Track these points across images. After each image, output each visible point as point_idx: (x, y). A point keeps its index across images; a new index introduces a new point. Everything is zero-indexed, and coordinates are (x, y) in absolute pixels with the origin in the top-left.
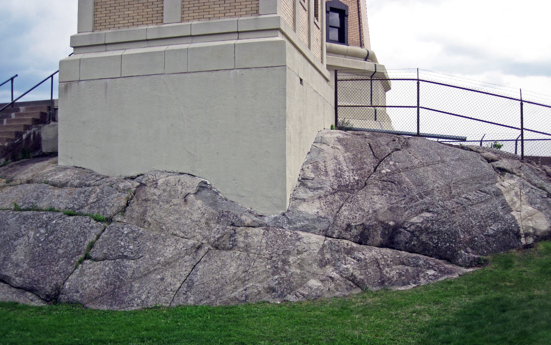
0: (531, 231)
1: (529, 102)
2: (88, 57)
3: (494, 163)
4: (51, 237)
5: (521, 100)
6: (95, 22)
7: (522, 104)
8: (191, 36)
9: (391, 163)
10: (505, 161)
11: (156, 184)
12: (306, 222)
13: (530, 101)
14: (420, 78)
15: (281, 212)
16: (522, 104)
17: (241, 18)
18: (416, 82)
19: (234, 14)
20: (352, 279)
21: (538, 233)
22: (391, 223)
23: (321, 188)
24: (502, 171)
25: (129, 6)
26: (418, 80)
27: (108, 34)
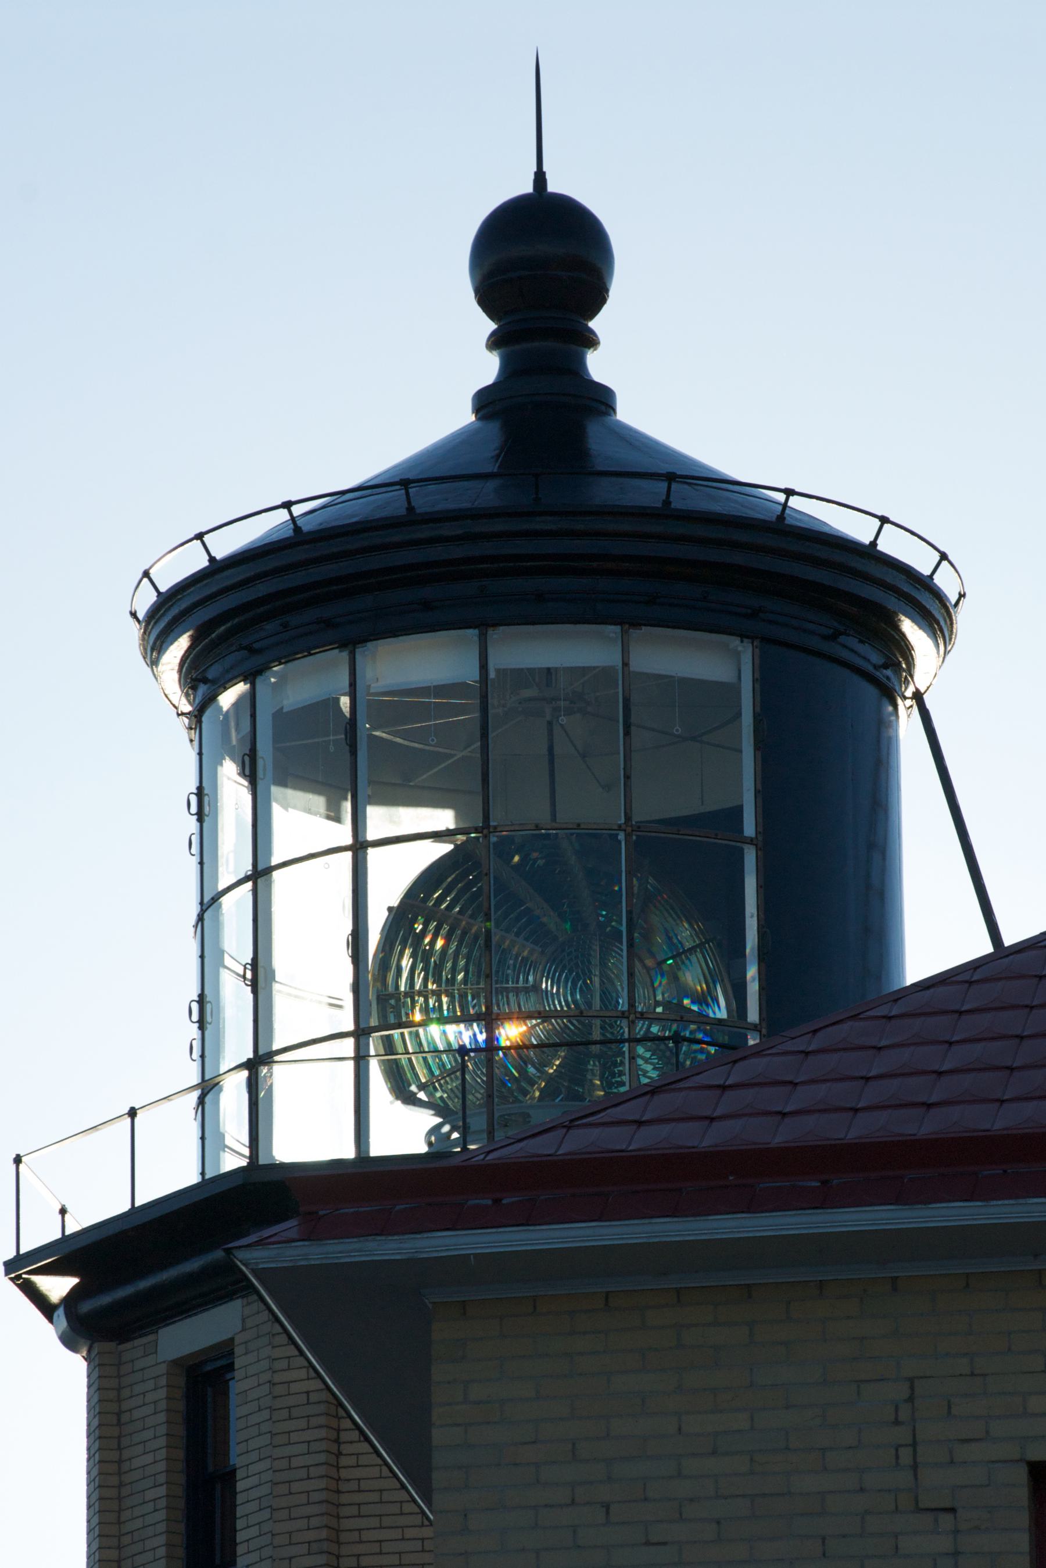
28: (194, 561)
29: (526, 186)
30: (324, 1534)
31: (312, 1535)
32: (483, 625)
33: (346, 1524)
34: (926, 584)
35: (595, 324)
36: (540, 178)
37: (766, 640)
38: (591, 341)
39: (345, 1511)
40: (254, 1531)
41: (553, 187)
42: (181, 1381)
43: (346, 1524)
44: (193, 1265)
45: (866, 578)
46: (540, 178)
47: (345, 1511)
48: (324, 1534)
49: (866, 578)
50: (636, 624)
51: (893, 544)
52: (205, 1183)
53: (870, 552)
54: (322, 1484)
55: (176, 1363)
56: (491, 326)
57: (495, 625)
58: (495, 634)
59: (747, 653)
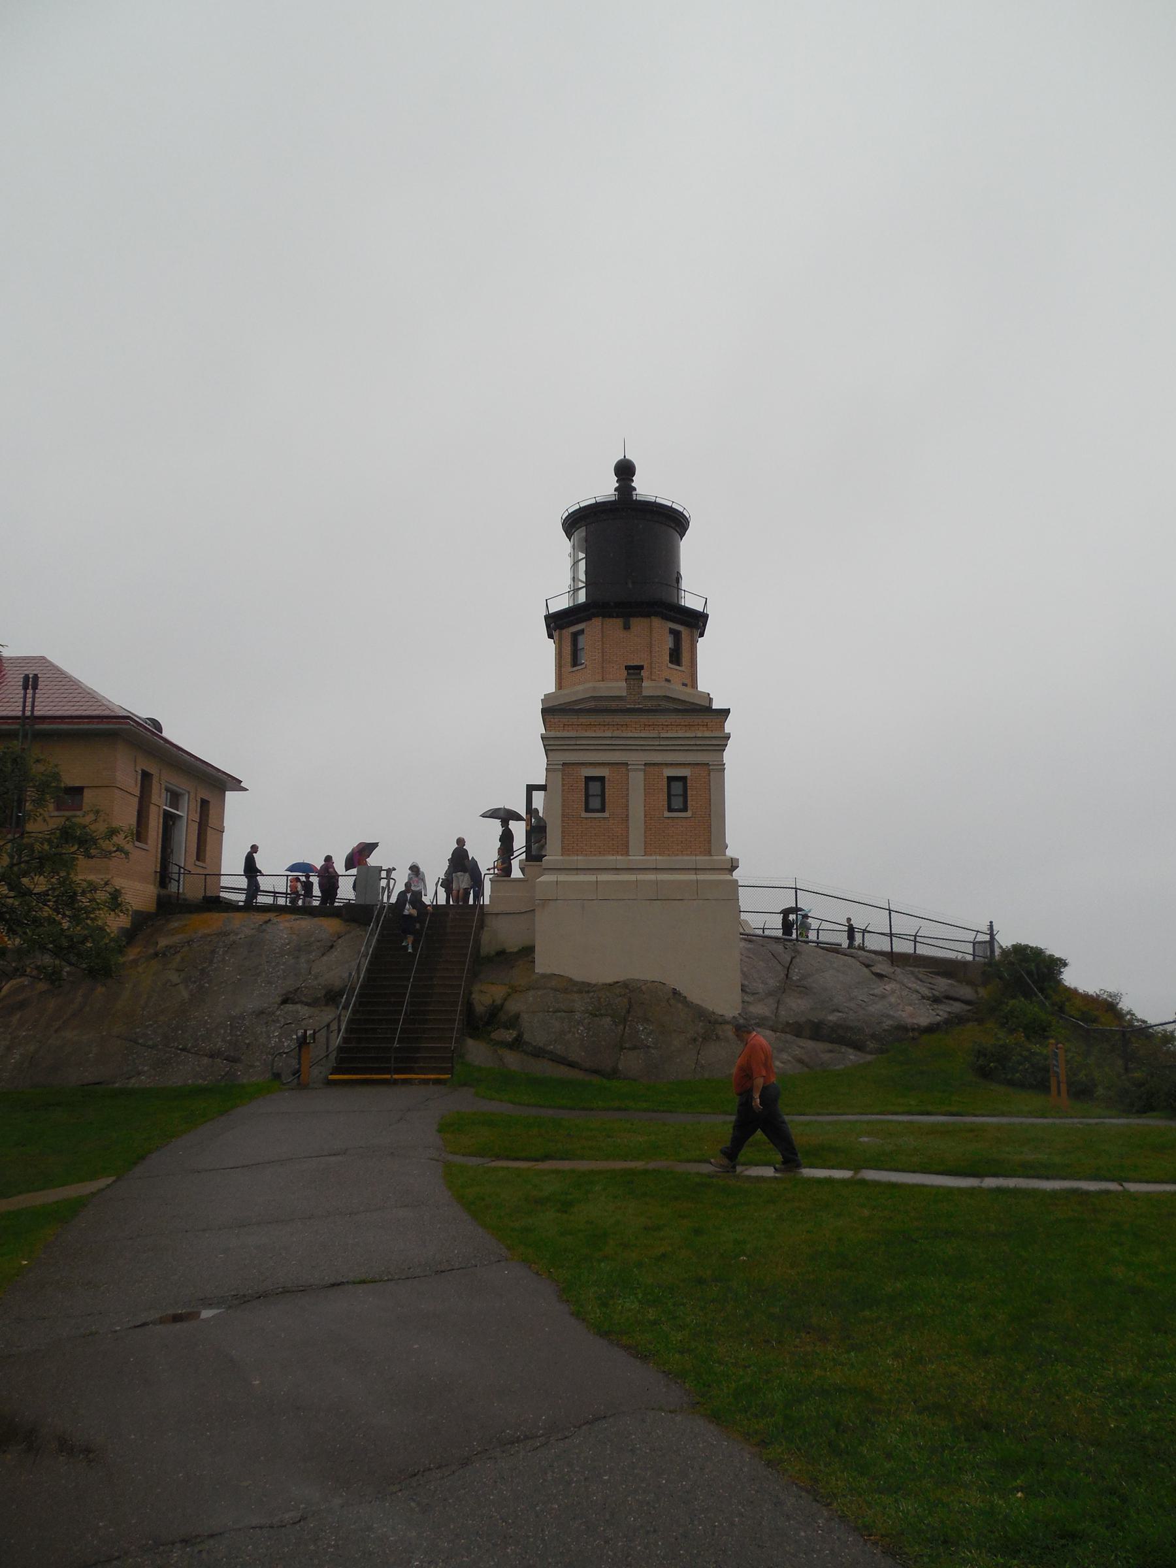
0: (916, 1027)
1: (896, 912)
2: (565, 880)
3: (873, 969)
4: (591, 1033)
5: (890, 910)
6: (563, 848)
7: (890, 913)
8: (656, 869)
9: (796, 970)
10: (879, 966)
11: (642, 990)
12: (757, 1020)
13: (897, 910)
14: (798, 887)
15: (738, 1012)
16: (890, 913)
17: (698, 858)
18: (794, 890)
19: (689, 853)
20: (800, 1061)
21: (922, 1028)
22: (816, 1020)
23: (757, 993)
24: (880, 976)
25: (595, 837)
26: (796, 888)
27: (579, 860)
28: (577, 507)
35: (634, 478)
36: (625, 456)
38: (633, 481)
41: (627, 457)
46: (625, 456)
51: (685, 513)
53: (682, 513)
55: (571, 633)
56: (616, 478)
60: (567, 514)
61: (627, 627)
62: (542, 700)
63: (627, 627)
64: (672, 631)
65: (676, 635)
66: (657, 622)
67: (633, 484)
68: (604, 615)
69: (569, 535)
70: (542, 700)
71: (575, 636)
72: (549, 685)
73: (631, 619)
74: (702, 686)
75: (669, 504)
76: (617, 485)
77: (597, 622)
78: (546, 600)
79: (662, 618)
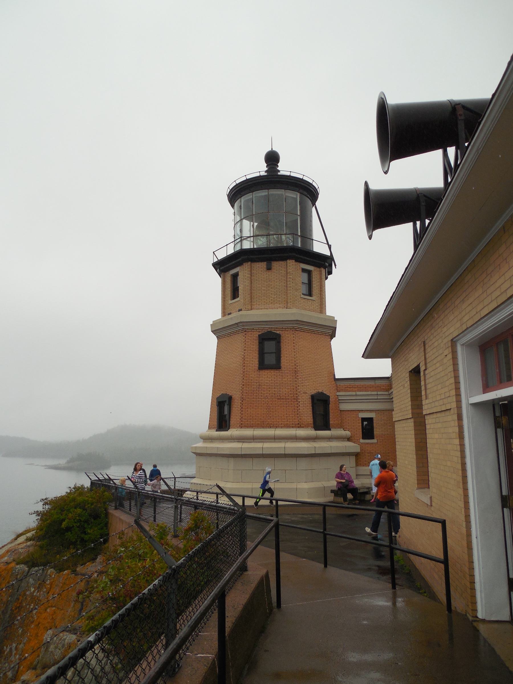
28: (234, 184)
29: (271, 149)
30: (250, 293)
31: (248, 293)
32: (268, 189)
33: (252, 292)
34: (317, 190)
36: (272, 149)
37: (300, 193)
39: (252, 290)
40: (241, 293)
41: (273, 149)
42: (232, 277)
43: (252, 292)
44: (234, 262)
45: (311, 187)
46: (272, 149)
47: (252, 290)
48: (250, 293)
49: (311, 187)
50: (286, 189)
51: (314, 184)
52: (235, 252)
53: (312, 184)
54: (250, 287)
57: (270, 189)
58: (269, 190)
59: (298, 194)
60: (229, 190)
61: (269, 268)
62: (211, 325)
63: (269, 268)
64: (304, 270)
65: (309, 272)
66: (291, 263)
67: (278, 169)
68: (253, 261)
69: (233, 206)
70: (211, 325)
71: (235, 277)
72: (217, 315)
73: (273, 262)
74: (330, 311)
75: (301, 177)
76: (267, 169)
77: (247, 266)
78: (214, 252)
79: (296, 261)
